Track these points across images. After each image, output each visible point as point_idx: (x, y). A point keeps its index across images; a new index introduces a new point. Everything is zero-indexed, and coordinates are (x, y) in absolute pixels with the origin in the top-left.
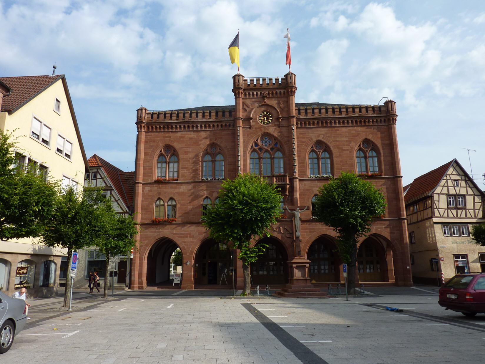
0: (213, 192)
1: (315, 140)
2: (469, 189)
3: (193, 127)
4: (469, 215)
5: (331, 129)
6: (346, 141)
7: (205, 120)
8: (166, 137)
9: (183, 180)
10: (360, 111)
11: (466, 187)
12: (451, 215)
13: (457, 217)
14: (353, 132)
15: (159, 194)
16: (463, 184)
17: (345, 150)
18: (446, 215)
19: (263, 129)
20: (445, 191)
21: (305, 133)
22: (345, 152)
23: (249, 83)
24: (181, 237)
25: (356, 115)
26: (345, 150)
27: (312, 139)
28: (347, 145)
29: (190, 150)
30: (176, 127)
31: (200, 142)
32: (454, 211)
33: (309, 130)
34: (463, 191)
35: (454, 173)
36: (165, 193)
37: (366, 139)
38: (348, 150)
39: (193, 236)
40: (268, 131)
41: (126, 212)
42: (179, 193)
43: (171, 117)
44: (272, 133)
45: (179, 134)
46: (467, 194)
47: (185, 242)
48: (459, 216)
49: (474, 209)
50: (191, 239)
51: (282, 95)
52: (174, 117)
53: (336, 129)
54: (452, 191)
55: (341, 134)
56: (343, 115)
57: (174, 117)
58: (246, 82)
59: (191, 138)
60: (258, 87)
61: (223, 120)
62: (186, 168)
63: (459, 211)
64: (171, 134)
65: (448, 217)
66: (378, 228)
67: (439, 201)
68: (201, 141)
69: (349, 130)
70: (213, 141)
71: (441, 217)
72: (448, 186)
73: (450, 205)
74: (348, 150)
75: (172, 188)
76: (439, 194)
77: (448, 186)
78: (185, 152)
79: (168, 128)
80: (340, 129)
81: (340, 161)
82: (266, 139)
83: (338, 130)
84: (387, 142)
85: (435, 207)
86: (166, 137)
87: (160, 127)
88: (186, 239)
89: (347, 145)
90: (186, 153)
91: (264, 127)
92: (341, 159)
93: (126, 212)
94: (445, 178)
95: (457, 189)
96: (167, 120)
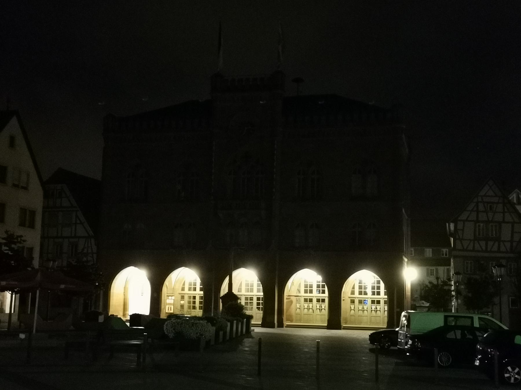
2: (507, 215)
4: (503, 249)
11: (504, 213)
12: (477, 246)
13: (486, 251)
16: (500, 207)
18: (470, 247)
20: (473, 216)
32: (483, 243)
34: (499, 217)
35: (491, 193)
46: (504, 222)
48: (489, 250)
49: (511, 241)
54: (483, 217)
63: (490, 243)
65: (473, 250)
67: (463, 230)
71: (463, 250)
72: (478, 212)
73: (479, 234)
76: (464, 221)
77: (478, 212)
85: (457, 237)
94: (475, 200)
95: (490, 215)
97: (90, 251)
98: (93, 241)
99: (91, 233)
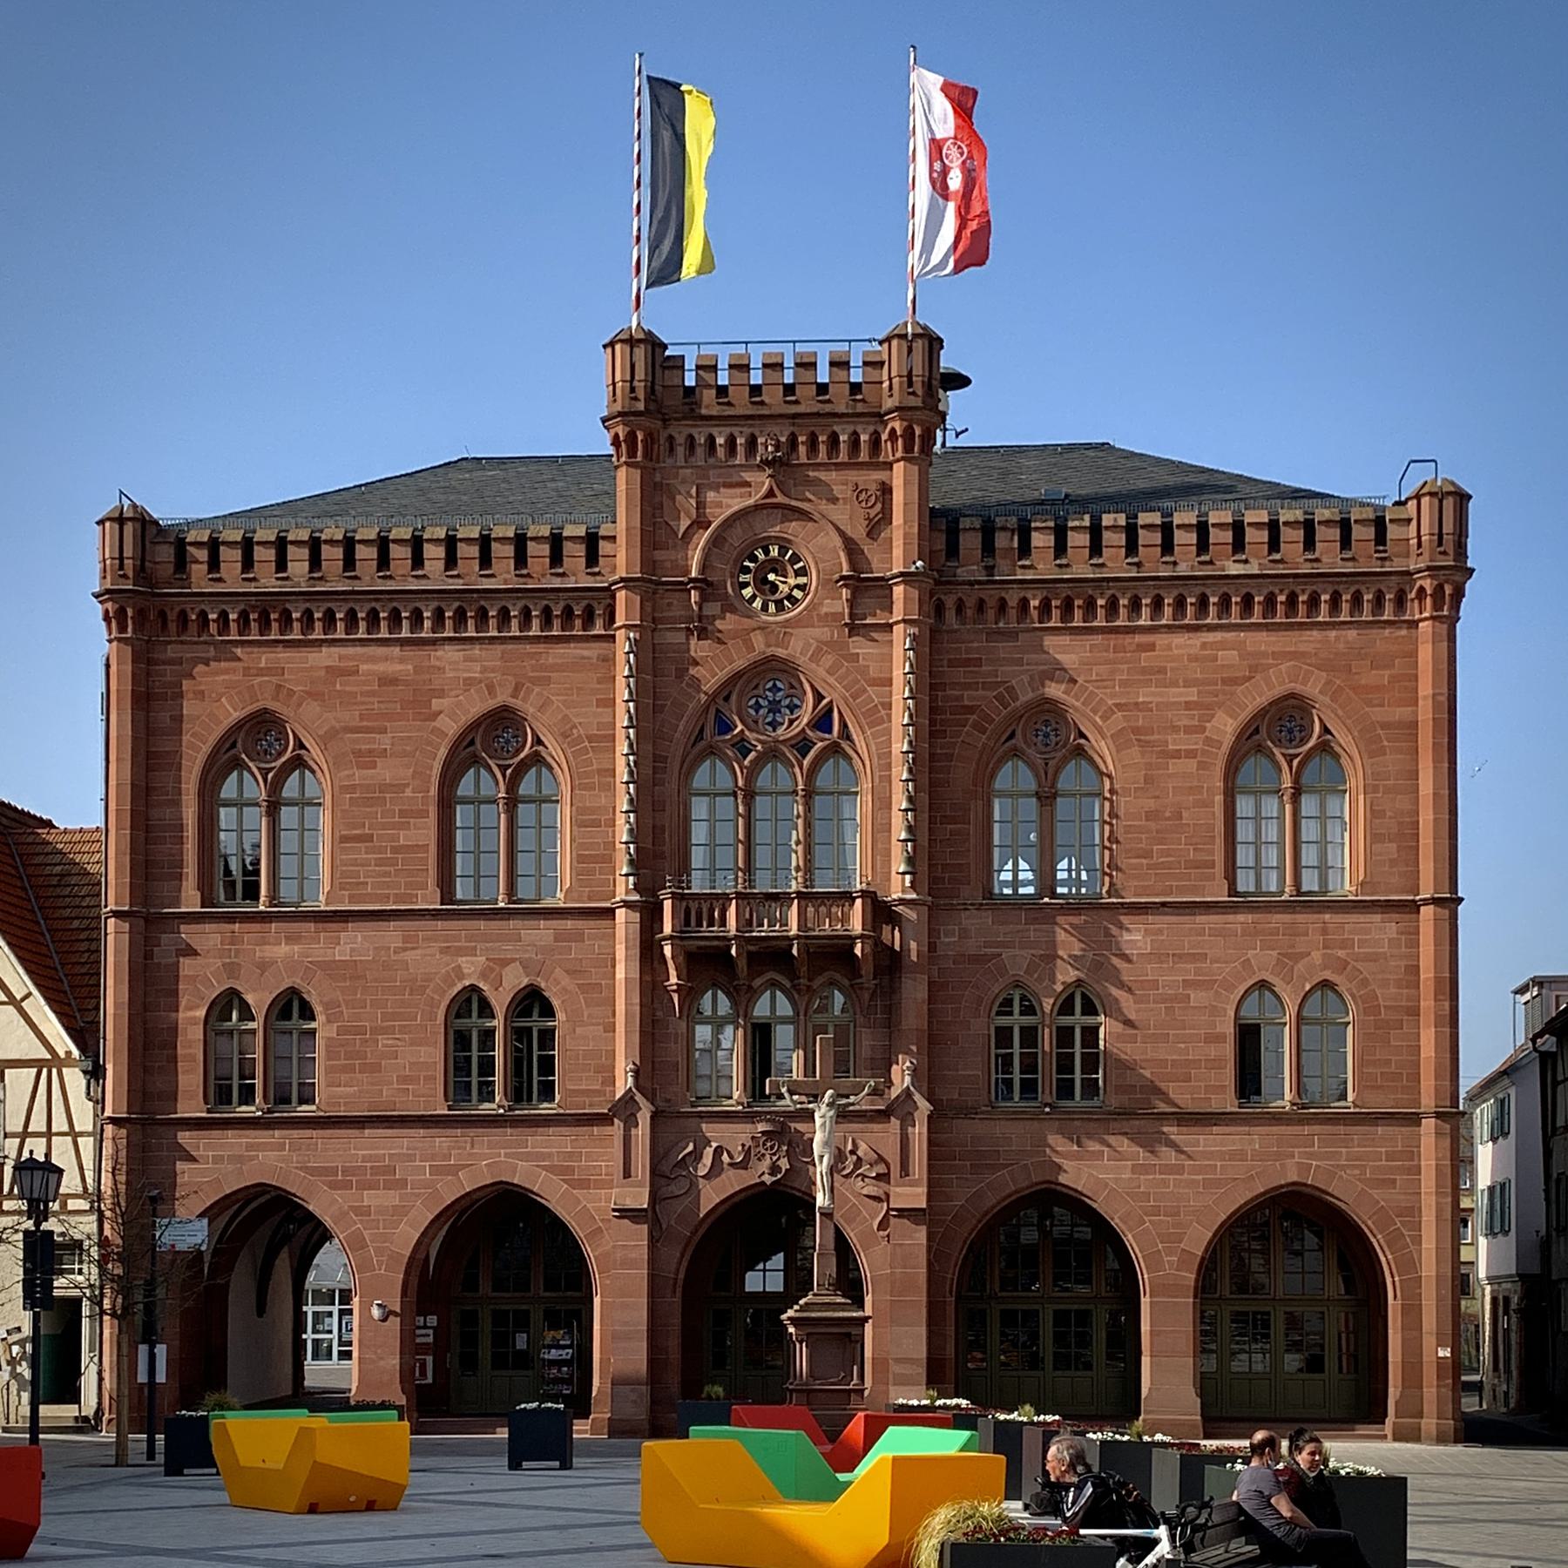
0: (505, 963)
1: (1026, 696)
3: (395, 619)
5: (1113, 640)
6: (1188, 705)
7: (457, 585)
8: (261, 672)
9: (352, 900)
10: (1274, 545)
14: (1231, 656)
15: (232, 970)
17: (1177, 755)
19: (758, 640)
21: (978, 662)
22: (1175, 766)
23: (690, 381)
24: (347, 1185)
25: (1253, 569)
26: (1177, 755)
27: (1011, 690)
28: (1189, 730)
29: (385, 742)
30: (308, 617)
31: (436, 704)
33: (1003, 648)
36: (263, 966)
37: (1292, 696)
38: (1191, 754)
39: (403, 1183)
40: (781, 652)
41: (68, 1061)
42: (330, 968)
43: (281, 564)
44: (802, 661)
45: (327, 657)
47: (363, 1211)
50: (392, 1198)
51: (864, 456)
52: (298, 564)
53: (1139, 638)
55: (1162, 671)
56: (1183, 569)
57: (298, 564)
58: (671, 378)
59: (387, 681)
60: (741, 403)
61: (557, 583)
62: (369, 838)
64: (283, 655)
66: (1311, 1156)
68: (441, 694)
69: (1204, 646)
70: (502, 698)
74: (1191, 754)
75: (290, 939)
78: (358, 754)
79: (265, 626)
80: (1161, 640)
81: (1151, 815)
82: (775, 689)
83: (1151, 647)
84: (1400, 713)
86: (261, 672)
87: (224, 615)
88: (369, 1198)
89: (1189, 730)
90: (366, 759)
91: (763, 628)
92: (1151, 804)
93: (68, 1061)
96: (268, 581)
97: (59, 1124)
98: (75, 1079)
99: (63, 1043)
